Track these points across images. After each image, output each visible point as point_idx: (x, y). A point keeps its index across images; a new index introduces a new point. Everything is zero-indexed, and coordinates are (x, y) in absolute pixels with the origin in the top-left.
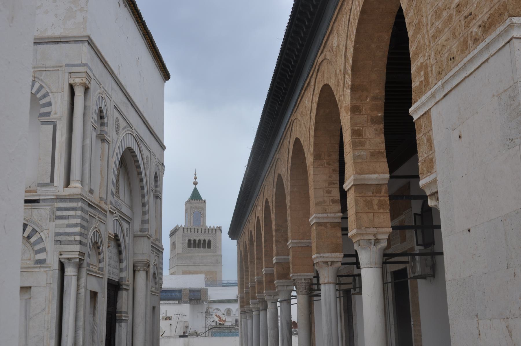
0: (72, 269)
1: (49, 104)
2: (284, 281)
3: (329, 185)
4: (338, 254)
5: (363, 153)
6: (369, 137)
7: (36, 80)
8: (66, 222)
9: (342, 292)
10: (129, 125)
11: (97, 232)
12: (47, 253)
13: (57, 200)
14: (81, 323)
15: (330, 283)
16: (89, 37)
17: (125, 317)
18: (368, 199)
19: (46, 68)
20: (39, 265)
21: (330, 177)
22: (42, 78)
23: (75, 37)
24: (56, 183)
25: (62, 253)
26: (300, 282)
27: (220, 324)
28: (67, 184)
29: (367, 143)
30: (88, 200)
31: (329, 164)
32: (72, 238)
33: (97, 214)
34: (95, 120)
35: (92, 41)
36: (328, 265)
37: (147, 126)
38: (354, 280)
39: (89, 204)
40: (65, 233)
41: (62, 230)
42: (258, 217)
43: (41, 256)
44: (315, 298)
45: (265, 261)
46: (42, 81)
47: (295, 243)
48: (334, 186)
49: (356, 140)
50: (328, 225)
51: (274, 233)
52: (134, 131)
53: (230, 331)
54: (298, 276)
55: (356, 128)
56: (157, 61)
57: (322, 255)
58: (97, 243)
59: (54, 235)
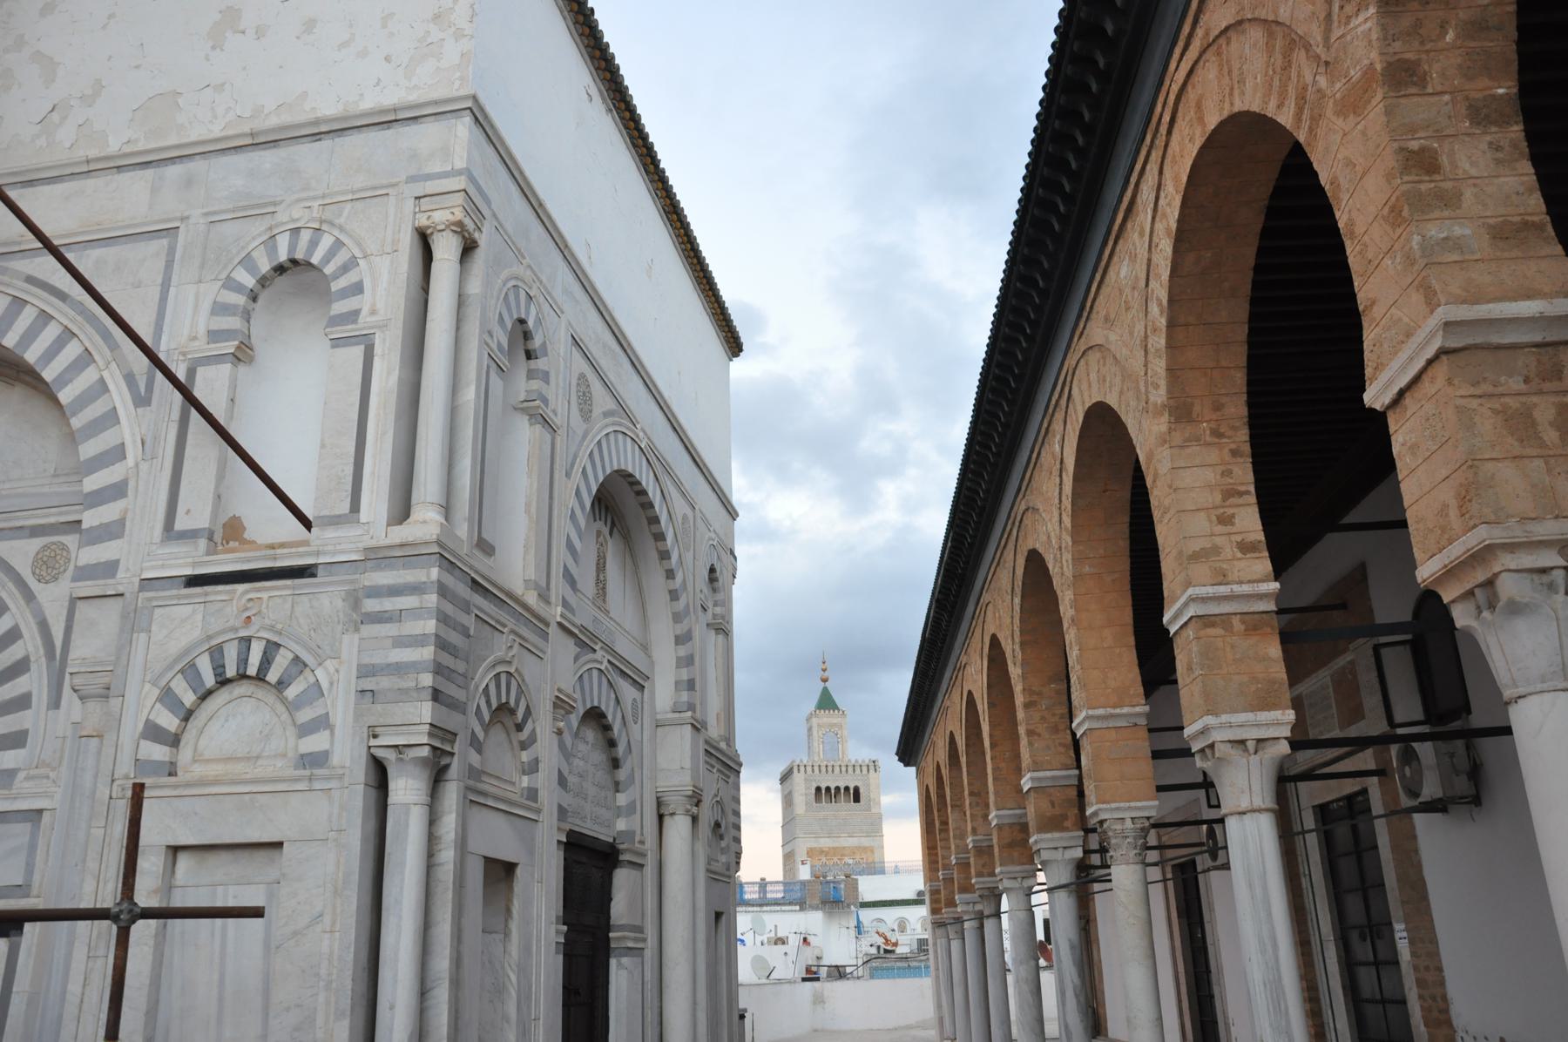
0: (410, 782)
1: (358, 289)
2: (1057, 835)
3: (1225, 499)
4: (1276, 715)
5: (1458, 231)
6: (1474, 172)
8: (390, 630)
9: (1169, 869)
11: (506, 677)
12: (332, 734)
13: (369, 564)
14: (442, 964)
15: (1259, 811)
16: (475, 98)
17: (636, 940)
18: (1513, 403)
19: (353, 192)
20: (307, 772)
21: (1227, 473)
22: (342, 221)
23: (436, 103)
24: (364, 515)
25: (378, 730)
26: (1118, 827)
28: (402, 511)
29: (1468, 194)
30: (471, 567)
31: (1216, 433)
33: (511, 623)
34: (499, 345)
35: (482, 110)
36: (1246, 750)
38: (1211, 834)
39: (474, 581)
40: (389, 665)
41: (377, 659)
42: (970, 693)
43: (315, 743)
44: (1097, 887)
45: (996, 793)
46: (341, 229)
47: (1099, 718)
48: (1240, 501)
49: (1423, 187)
50: (1236, 621)
51: (1020, 714)
54: (1112, 810)
55: (1414, 145)
57: (1224, 718)
58: (513, 712)
59: (354, 673)
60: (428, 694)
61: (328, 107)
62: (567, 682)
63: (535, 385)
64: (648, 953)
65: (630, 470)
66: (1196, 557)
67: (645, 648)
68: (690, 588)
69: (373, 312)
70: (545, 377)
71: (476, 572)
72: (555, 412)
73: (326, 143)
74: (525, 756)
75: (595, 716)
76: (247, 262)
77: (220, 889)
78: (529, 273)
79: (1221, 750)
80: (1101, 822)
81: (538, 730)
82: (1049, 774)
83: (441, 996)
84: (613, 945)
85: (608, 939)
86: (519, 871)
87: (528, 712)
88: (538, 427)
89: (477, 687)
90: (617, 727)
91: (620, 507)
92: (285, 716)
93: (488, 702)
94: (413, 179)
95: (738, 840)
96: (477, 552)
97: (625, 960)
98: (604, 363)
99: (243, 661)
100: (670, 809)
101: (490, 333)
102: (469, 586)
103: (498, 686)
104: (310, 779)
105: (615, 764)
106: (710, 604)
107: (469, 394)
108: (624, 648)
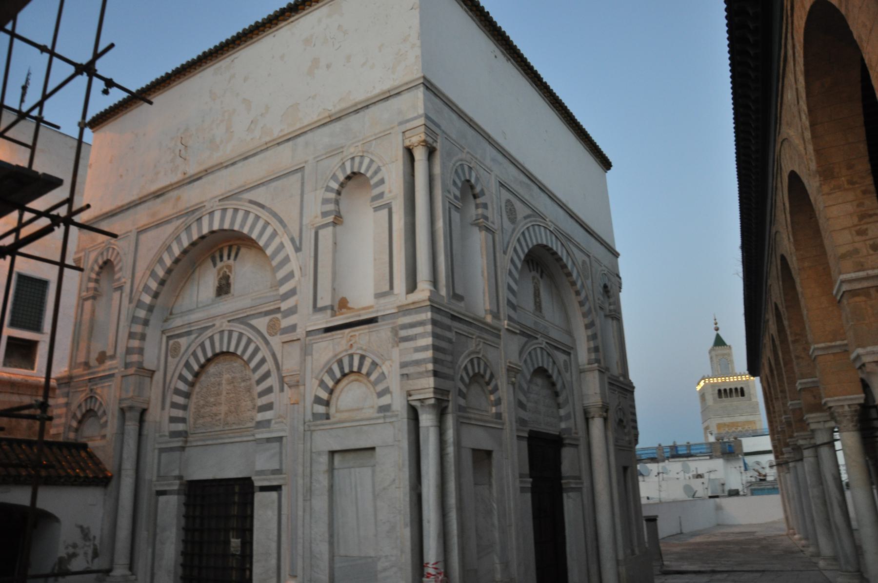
1: (382, 182)
2: (818, 414)
7: (365, 154)
10: (536, 213)
13: (400, 314)
14: (452, 500)
16: (424, 78)
17: (576, 484)
20: (382, 415)
21: (860, 205)
23: (407, 84)
25: (412, 392)
26: (840, 410)
27: (761, 480)
28: (412, 286)
30: (450, 309)
31: (850, 182)
32: (422, 369)
33: (477, 333)
34: (456, 197)
35: (429, 82)
37: (577, 221)
43: (385, 400)
46: (372, 154)
50: (873, 292)
52: (550, 224)
53: (772, 489)
54: (835, 401)
56: (585, 142)
57: (869, 349)
58: (483, 376)
59: (398, 366)
60: (431, 374)
61: (360, 95)
62: (514, 358)
63: (480, 211)
64: (585, 490)
65: (545, 243)
66: (843, 256)
67: (570, 333)
68: (591, 298)
69: (390, 192)
70: (485, 206)
71: (454, 311)
72: (493, 223)
73: (362, 114)
74: (492, 398)
75: (541, 372)
76: (334, 177)
77: (353, 470)
78: (469, 156)
79: (869, 368)
80: (830, 408)
81: (499, 384)
82: (810, 380)
83: (453, 516)
84: (564, 486)
85: (561, 484)
86: (494, 455)
87: (492, 376)
88: (484, 232)
89: (460, 367)
90: (555, 377)
91: (541, 262)
92: (372, 389)
93: (467, 374)
94: (400, 124)
95: (636, 428)
96: (454, 301)
97: (571, 494)
98: (521, 191)
99: (361, 365)
100: (592, 415)
101: (449, 192)
102: (450, 321)
103: (473, 365)
104: (384, 417)
105: (557, 394)
106: (606, 305)
107: (440, 224)
108: (555, 334)
